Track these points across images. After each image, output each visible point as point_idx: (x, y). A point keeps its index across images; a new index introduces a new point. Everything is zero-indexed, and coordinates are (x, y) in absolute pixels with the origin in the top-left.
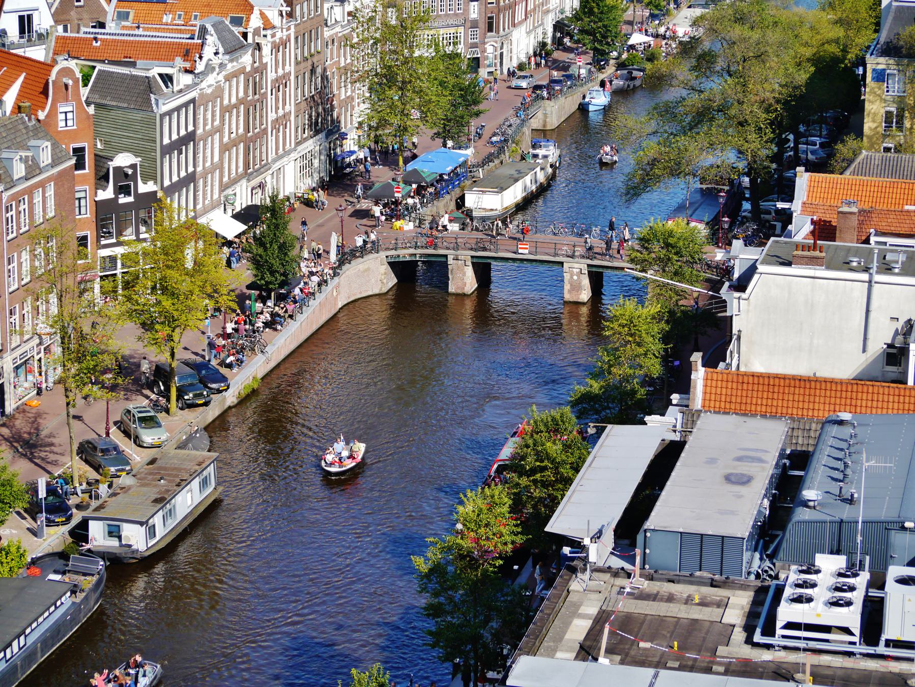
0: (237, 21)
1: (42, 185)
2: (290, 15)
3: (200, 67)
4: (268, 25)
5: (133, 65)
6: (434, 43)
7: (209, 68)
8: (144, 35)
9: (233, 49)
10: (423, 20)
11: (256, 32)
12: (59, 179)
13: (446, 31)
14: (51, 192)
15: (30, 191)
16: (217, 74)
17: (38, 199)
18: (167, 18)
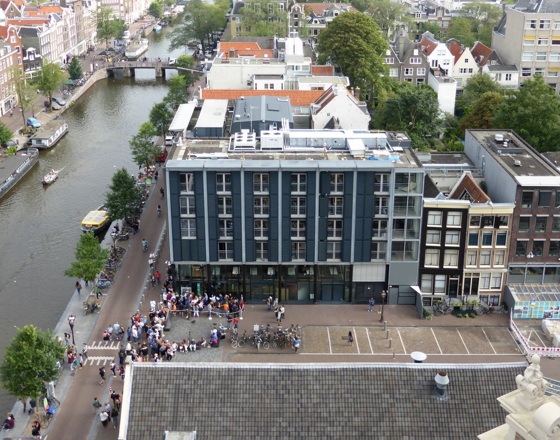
0: (59, 14)
1: (9, 57)
2: (73, 12)
3: (50, 25)
4: (68, 14)
5: (31, 26)
6: (114, 17)
7: (52, 26)
8: (32, 18)
9: (58, 20)
10: (111, 11)
11: (65, 16)
12: (13, 55)
13: (116, 13)
14: (11, 59)
15: (5, 59)
16: (55, 27)
17: (8, 61)
18: (38, 14)
